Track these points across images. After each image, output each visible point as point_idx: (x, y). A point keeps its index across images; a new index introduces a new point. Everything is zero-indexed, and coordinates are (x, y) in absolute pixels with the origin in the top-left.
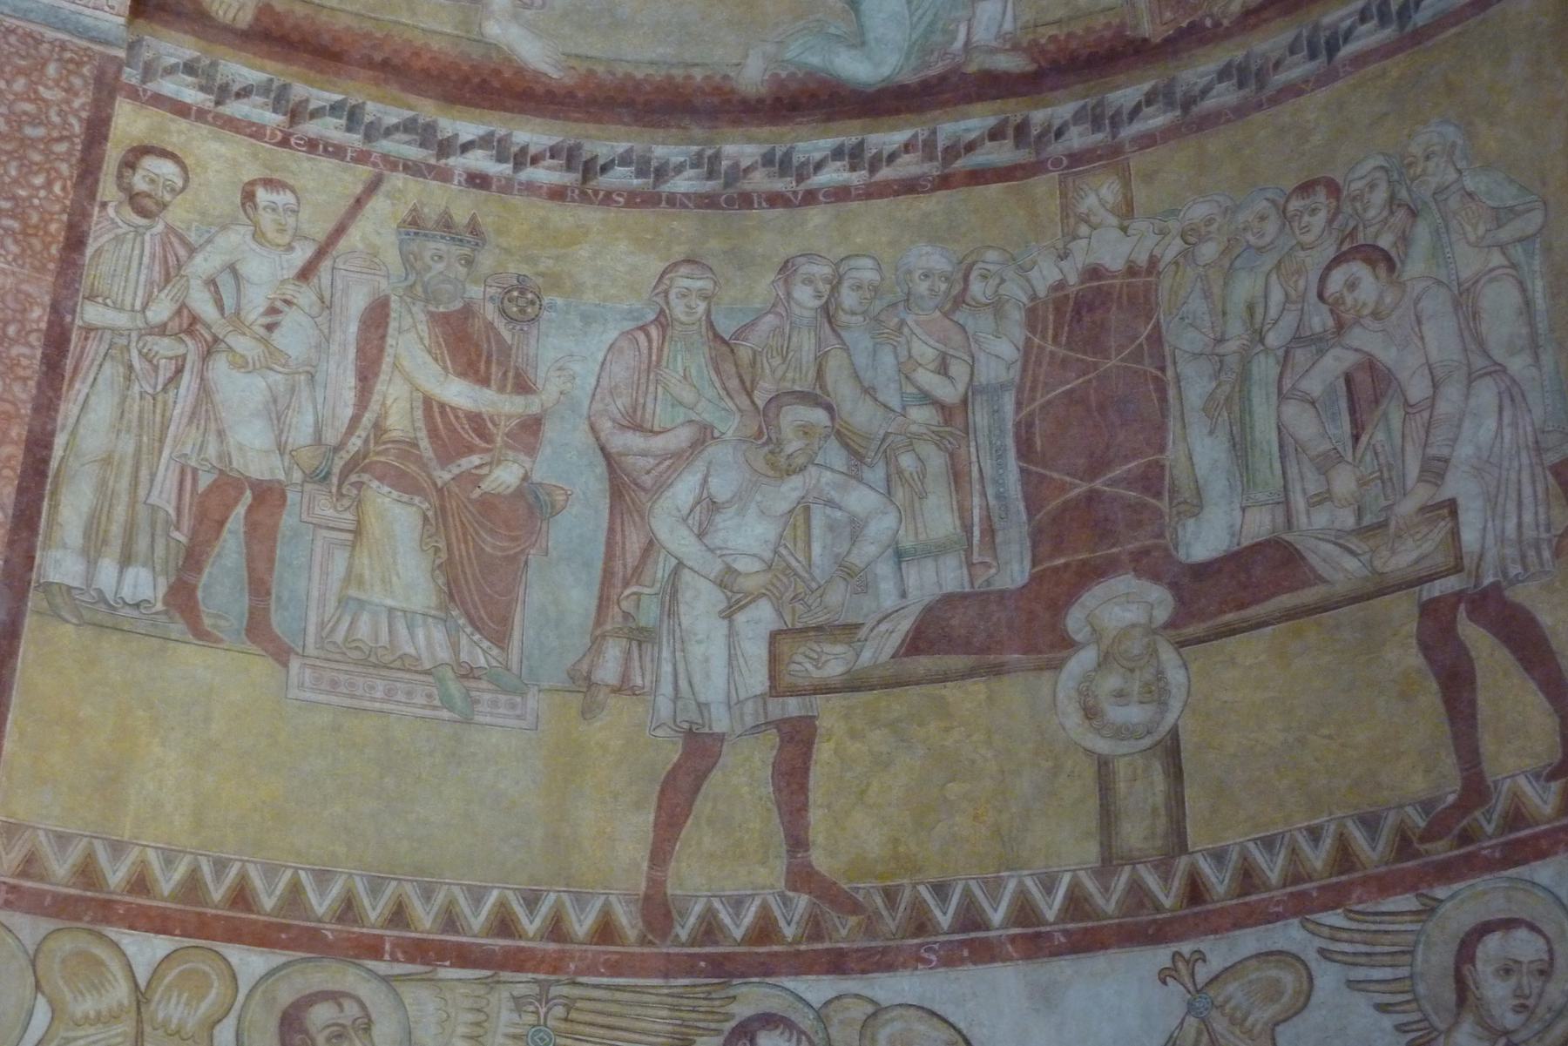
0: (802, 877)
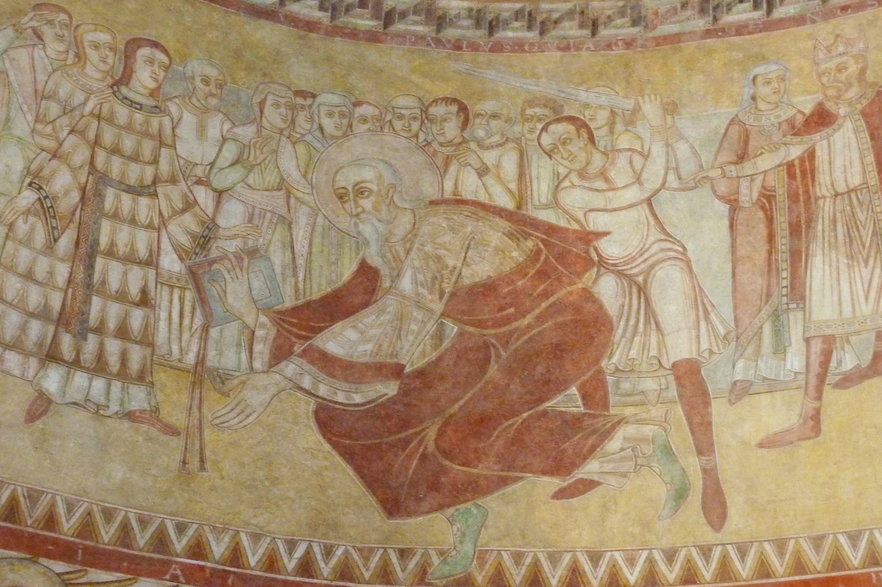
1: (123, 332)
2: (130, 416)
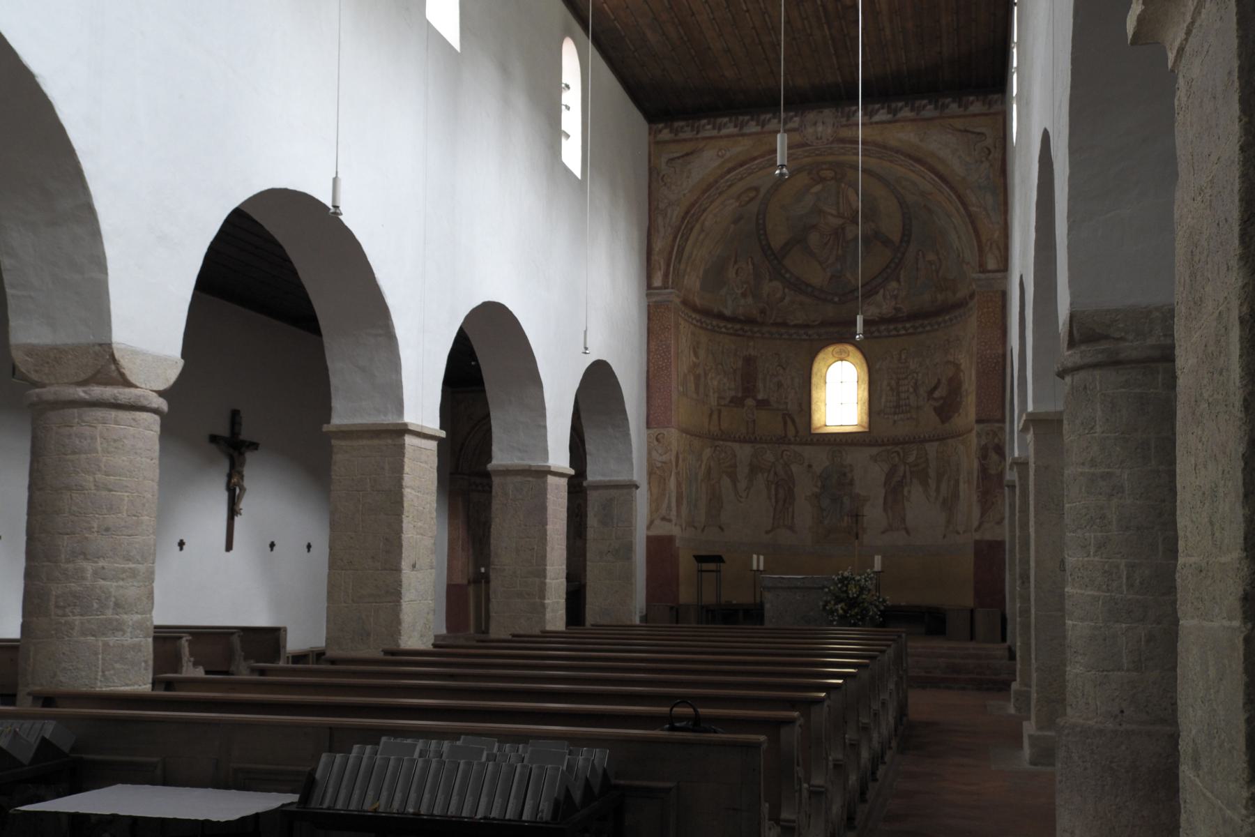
0: (720, 429)
1: (906, 405)
2: (908, 419)
